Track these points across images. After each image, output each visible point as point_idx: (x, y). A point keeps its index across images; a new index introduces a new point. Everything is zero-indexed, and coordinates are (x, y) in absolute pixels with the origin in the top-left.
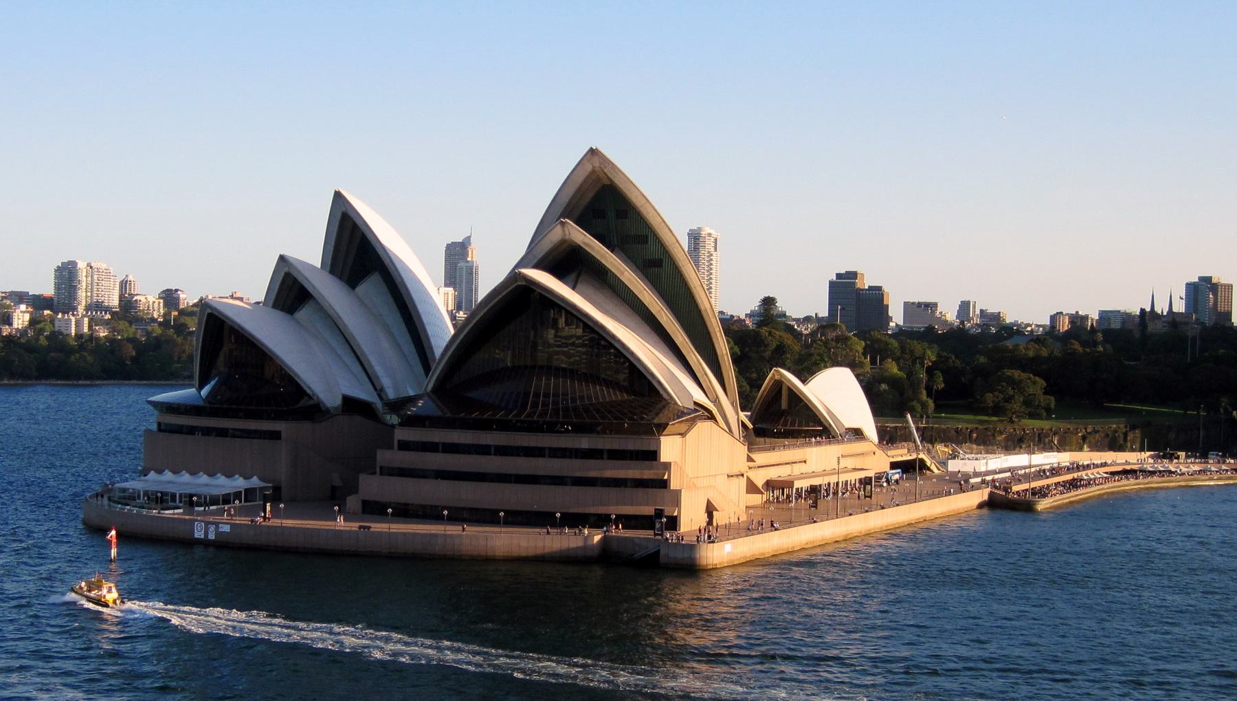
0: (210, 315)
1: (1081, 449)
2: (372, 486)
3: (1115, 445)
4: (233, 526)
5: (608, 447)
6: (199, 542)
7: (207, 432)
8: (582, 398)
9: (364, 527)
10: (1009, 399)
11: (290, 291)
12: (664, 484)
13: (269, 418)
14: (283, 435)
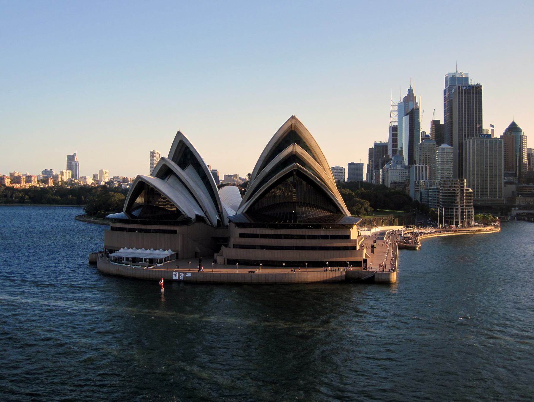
0: (140, 181)
1: (382, 225)
2: (228, 252)
3: (391, 224)
4: (192, 273)
5: (331, 234)
6: (175, 281)
7: (140, 231)
8: (315, 214)
9: (251, 272)
10: (360, 209)
11: (164, 172)
12: (354, 248)
13: (171, 225)
14: (178, 232)
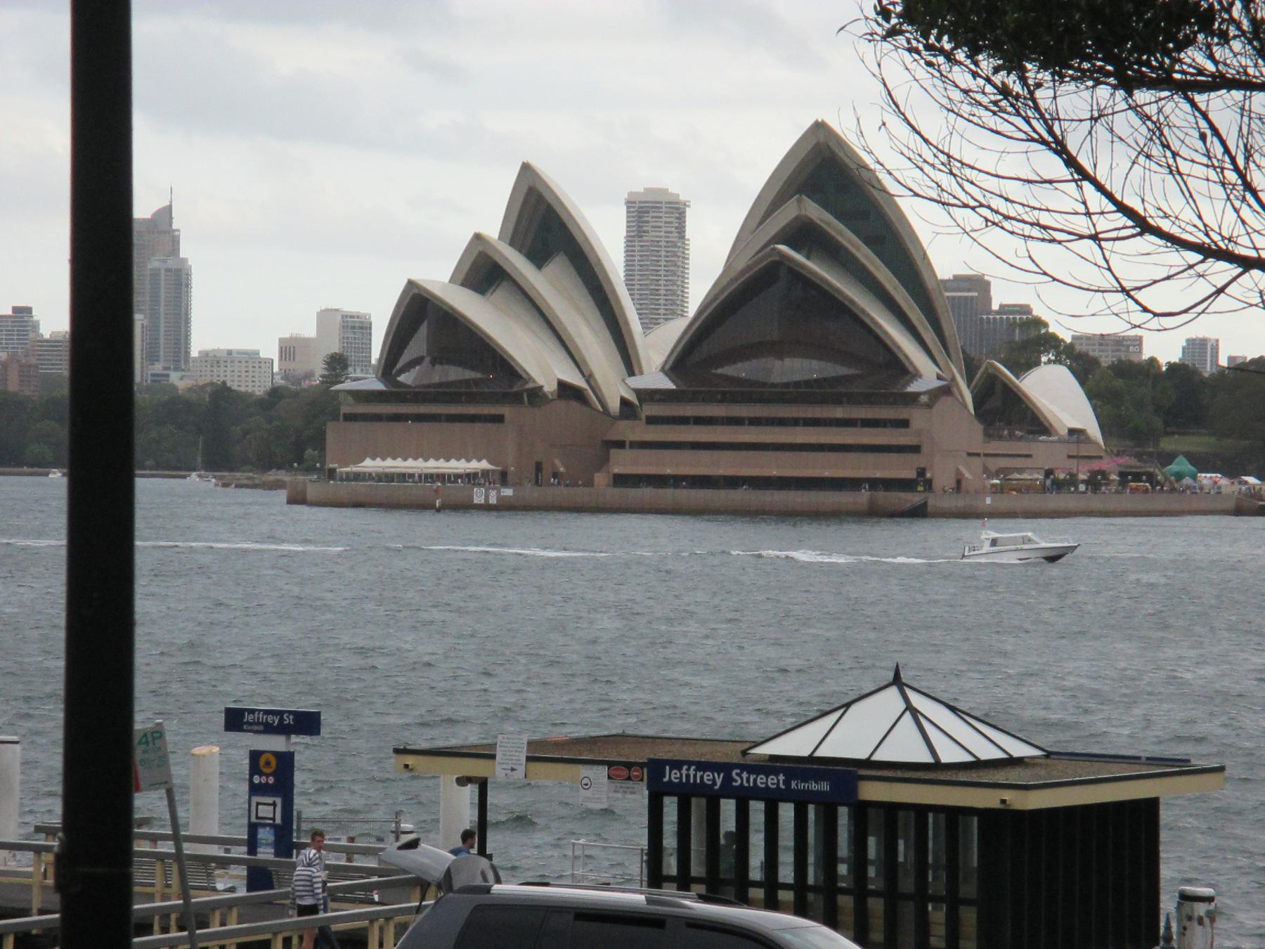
11: (483, 272)
